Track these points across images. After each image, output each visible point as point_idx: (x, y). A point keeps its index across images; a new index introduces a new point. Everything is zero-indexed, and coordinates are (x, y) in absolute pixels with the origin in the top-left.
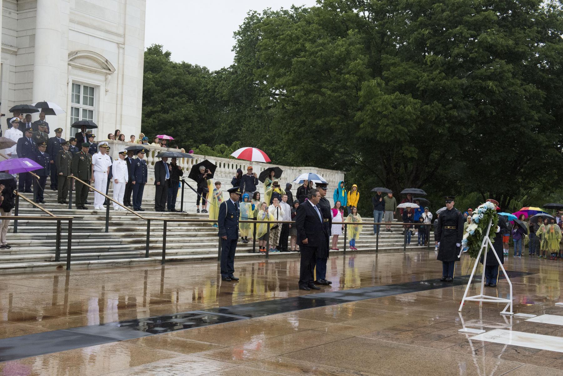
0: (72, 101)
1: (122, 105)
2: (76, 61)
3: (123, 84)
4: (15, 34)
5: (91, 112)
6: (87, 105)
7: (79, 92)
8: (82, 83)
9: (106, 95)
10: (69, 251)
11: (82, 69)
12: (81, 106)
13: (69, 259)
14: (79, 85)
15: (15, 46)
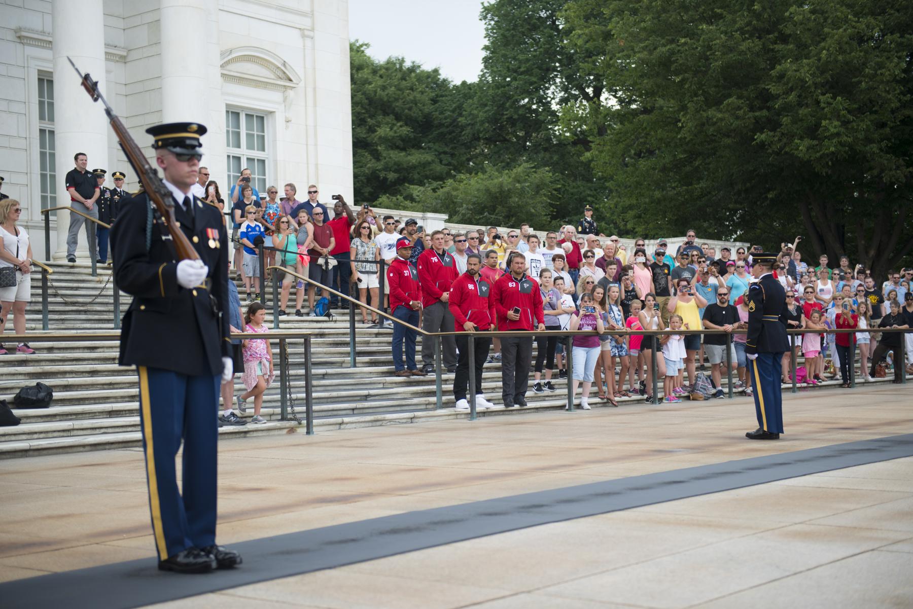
0: (228, 145)
1: (316, 145)
2: (230, 67)
3: (315, 105)
4: (121, 24)
5: (263, 162)
6: (254, 149)
7: (238, 127)
8: (243, 108)
9: (287, 127)
10: (308, 401)
11: (240, 80)
12: (244, 152)
13: (309, 414)
14: (238, 114)
15: (122, 45)
